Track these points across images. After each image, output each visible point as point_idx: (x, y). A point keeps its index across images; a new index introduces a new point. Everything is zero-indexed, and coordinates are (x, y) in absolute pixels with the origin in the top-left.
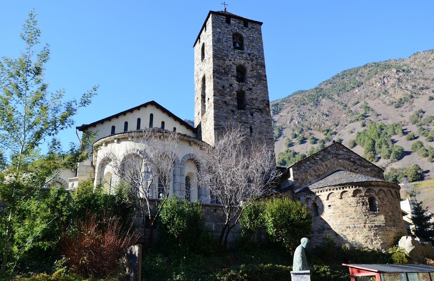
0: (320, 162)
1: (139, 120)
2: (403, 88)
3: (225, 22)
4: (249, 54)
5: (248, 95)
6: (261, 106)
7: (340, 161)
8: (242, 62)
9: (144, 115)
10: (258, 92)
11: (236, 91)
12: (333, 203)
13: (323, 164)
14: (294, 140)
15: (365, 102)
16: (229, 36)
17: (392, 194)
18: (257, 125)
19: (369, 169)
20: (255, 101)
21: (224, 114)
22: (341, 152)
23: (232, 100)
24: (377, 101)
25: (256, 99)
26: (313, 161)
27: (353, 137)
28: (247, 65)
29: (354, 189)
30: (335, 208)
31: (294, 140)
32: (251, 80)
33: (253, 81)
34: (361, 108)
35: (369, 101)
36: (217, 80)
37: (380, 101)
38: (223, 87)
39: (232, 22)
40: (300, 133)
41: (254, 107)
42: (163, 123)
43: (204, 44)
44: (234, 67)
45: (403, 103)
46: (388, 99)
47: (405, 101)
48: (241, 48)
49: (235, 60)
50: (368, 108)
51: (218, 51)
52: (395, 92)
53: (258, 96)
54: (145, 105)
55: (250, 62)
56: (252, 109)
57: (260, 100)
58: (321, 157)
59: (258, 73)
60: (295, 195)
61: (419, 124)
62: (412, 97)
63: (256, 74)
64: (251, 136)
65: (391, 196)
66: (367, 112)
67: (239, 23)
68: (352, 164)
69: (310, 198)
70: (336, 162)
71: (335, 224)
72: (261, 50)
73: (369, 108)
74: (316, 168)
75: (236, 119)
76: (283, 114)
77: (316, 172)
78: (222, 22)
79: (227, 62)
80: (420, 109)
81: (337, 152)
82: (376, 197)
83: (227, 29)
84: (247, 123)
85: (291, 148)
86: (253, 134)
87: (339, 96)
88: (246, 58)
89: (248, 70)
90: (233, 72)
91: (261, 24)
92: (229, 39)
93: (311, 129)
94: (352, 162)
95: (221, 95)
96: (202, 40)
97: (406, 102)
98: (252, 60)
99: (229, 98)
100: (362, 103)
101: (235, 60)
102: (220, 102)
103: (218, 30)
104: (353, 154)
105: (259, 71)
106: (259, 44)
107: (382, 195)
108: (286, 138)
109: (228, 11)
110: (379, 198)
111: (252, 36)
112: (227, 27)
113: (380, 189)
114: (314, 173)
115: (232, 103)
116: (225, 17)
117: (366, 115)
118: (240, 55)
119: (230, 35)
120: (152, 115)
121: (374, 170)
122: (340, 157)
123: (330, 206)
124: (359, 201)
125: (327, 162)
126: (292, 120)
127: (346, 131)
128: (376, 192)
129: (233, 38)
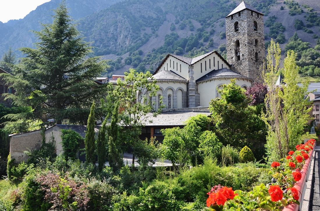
3: (251, 14)
4: (259, 33)
5: (259, 55)
8: (257, 38)
16: (252, 23)
31: (177, 26)
32: (259, 47)
36: (249, 47)
39: (253, 14)
40: (182, 20)
41: (261, 61)
42: (218, 61)
45: (262, 8)
47: (264, 6)
56: (260, 62)
59: (262, 43)
61: (272, 27)
62: (269, 4)
67: (256, 15)
76: (168, 2)
79: (252, 38)
80: (273, 15)
83: (252, 19)
88: (258, 35)
90: (254, 43)
95: (251, 55)
96: (235, 20)
97: (264, 7)
98: (260, 36)
99: (253, 56)
103: (249, 19)
108: (170, 23)
112: (252, 18)
116: (251, 12)
118: (256, 34)
120: (214, 57)
126: (176, 7)
127: (219, 24)
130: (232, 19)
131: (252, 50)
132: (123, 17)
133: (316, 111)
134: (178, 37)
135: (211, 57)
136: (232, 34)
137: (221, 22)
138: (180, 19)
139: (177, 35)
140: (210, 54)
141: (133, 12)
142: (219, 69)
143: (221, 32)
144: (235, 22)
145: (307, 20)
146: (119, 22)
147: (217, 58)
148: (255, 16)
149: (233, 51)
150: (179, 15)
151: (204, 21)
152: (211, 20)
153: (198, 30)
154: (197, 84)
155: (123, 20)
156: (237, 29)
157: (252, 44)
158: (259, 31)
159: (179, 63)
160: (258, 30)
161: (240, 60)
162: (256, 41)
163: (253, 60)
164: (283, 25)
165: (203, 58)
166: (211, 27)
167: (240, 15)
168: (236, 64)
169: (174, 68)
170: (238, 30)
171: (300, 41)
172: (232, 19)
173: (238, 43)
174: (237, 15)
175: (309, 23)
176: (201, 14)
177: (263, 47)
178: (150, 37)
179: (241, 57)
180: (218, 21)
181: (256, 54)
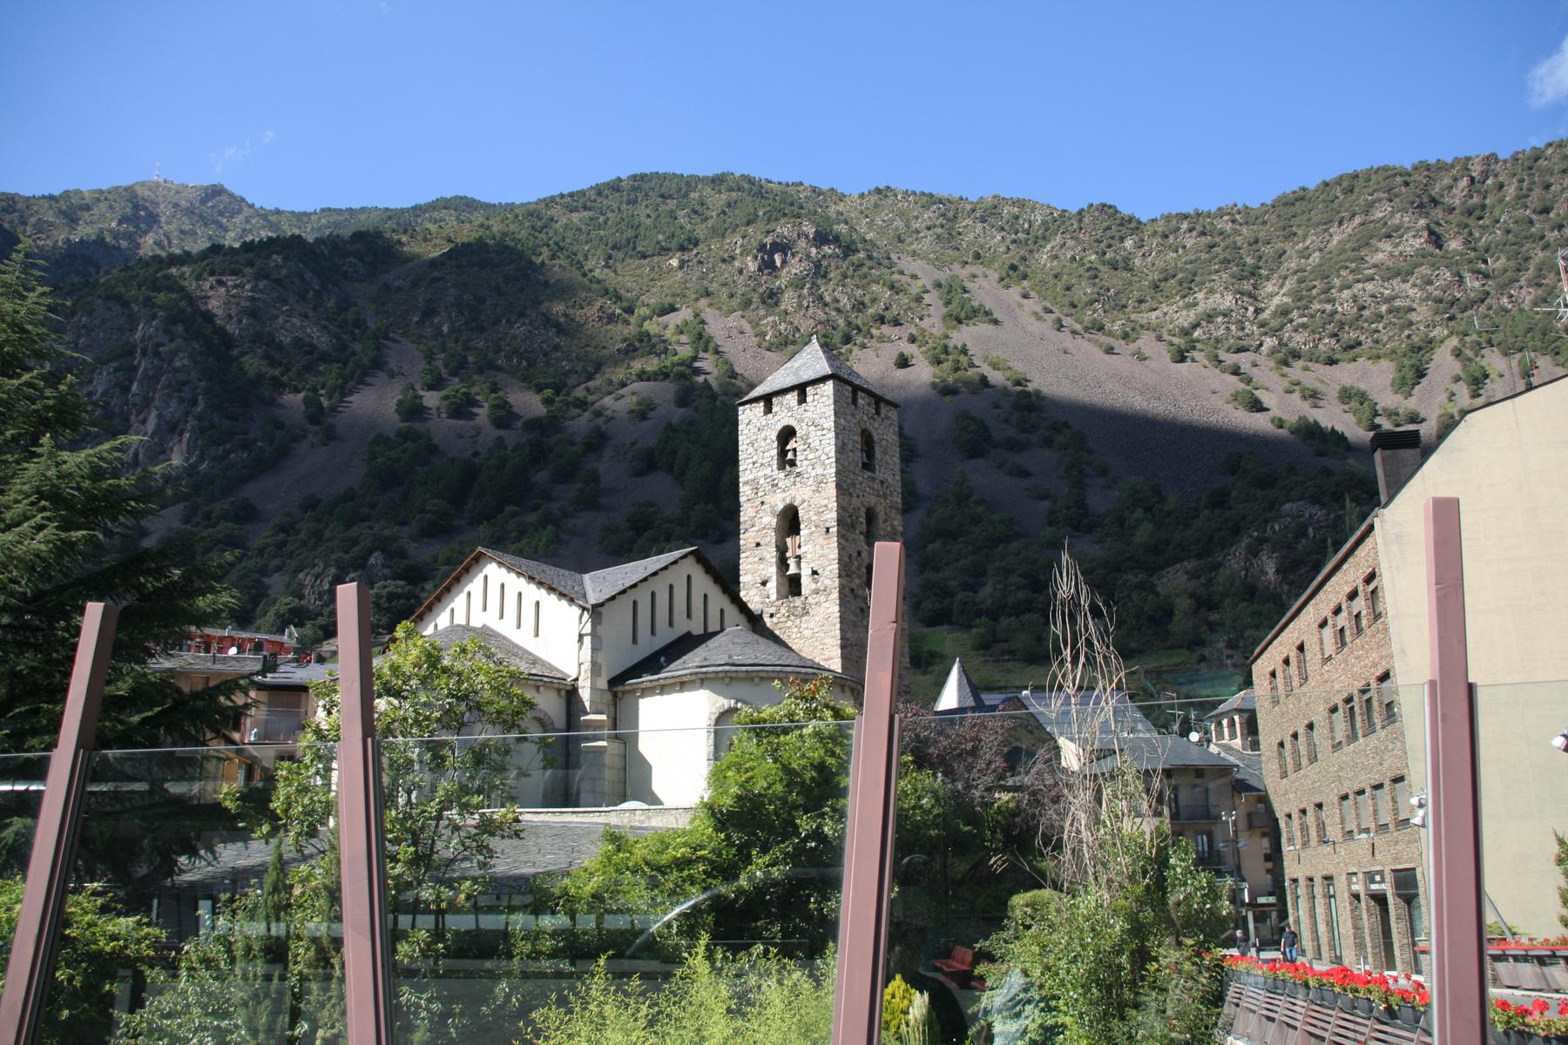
1: (671, 587)
2: (828, 299)
4: (882, 482)
8: (873, 500)
15: (697, 315)
21: (852, 617)
24: (734, 320)
28: (880, 510)
34: (682, 332)
35: (709, 314)
37: (747, 327)
39: (860, 401)
40: (454, 374)
46: (774, 325)
52: (800, 306)
62: (847, 339)
66: (701, 355)
73: (709, 340)
76: (397, 283)
79: (854, 500)
85: (417, 426)
87: (607, 266)
93: (499, 369)
100: (684, 314)
117: (697, 364)
130: (768, 410)
132: (167, 332)
134: (433, 449)
135: (677, 578)
136: (766, 477)
137: (635, 399)
138: (446, 366)
139: (430, 439)
140: (671, 559)
141: (219, 312)
142: (710, 630)
143: (633, 444)
144: (779, 427)
145: (1006, 421)
146: (144, 353)
147: (703, 583)
149: (771, 554)
152: (591, 384)
154: (615, 695)
155: (163, 345)
156: (790, 456)
157: (853, 526)
158: (879, 475)
159: (532, 592)
161: (799, 594)
162: (871, 516)
163: (856, 596)
165: (645, 579)
166: (587, 415)
167: (802, 400)
168: (783, 611)
169: (502, 617)
170: (793, 463)
171: (980, 509)
172: (768, 410)
173: (790, 521)
174: (792, 398)
175: (1012, 432)
176: (545, 355)
178: (295, 439)
179: (804, 580)
180: (622, 391)
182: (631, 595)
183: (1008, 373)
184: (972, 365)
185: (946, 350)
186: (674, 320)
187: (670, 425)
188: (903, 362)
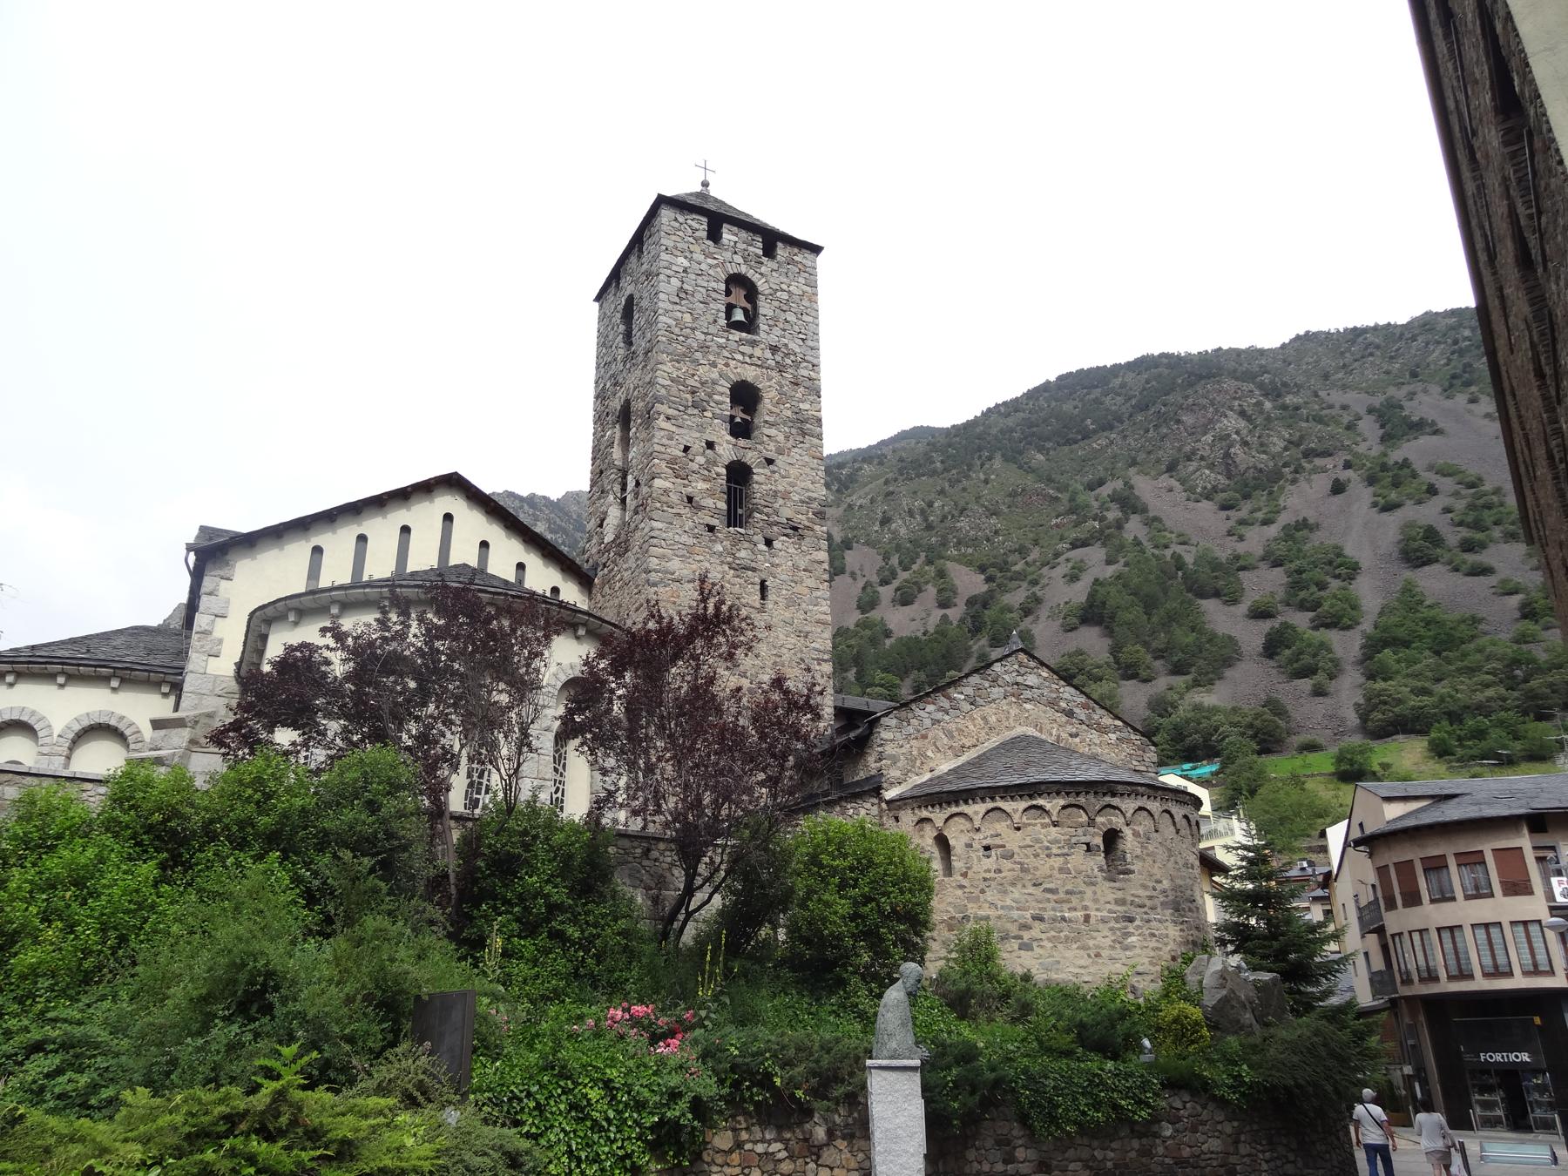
0: (966, 707)
4: (774, 349)
6: (802, 519)
7: (1028, 706)
8: (750, 374)
9: (425, 517)
10: (793, 471)
11: (727, 467)
12: (998, 841)
13: (977, 714)
14: (886, 592)
17: (1174, 824)
18: (783, 577)
19: (1113, 736)
20: (781, 501)
22: (1031, 680)
23: (711, 493)
24: (1166, 481)
25: (786, 496)
26: (946, 704)
27: (1078, 593)
29: (1062, 802)
30: (1003, 857)
32: (772, 432)
33: (781, 438)
38: (686, 449)
40: (905, 569)
43: (630, 299)
44: (724, 388)
47: (1256, 488)
48: (749, 325)
49: (727, 365)
50: (1128, 503)
51: (677, 331)
53: (790, 484)
54: (426, 489)
55: (774, 374)
57: (796, 498)
58: (969, 691)
60: (884, 805)
61: (1293, 566)
63: (789, 413)
64: (762, 610)
65: (1172, 829)
68: (1065, 719)
69: (928, 820)
70: (1014, 711)
71: (1000, 904)
72: (809, 337)
74: (952, 726)
75: (721, 554)
77: (950, 735)
78: (697, 234)
81: (1020, 679)
82: (1127, 832)
83: (710, 261)
84: (754, 570)
86: (770, 605)
89: (766, 401)
91: (816, 249)
92: (714, 295)
94: (1063, 711)
96: (628, 287)
98: (781, 369)
99: (701, 485)
101: (727, 365)
102: (674, 498)
103: (681, 260)
104: (1068, 689)
105: (802, 406)
106: (805, 318)
107: (1144, 824)
108: (861, 584)
109: (714, 192)
110: (1136, 834)
111: (784, 287)
113: (1141, 809)
114: (946, 740)
115: (709, 502)
116: (705, 219)
118: (747, 349)
119: (717, 281)
120: (448, 518)
121: (1129, 741)
122: (1028, 694)
123: (987, 848)
124: (1074, 840)
125: (989, 710)
128: (1129, 815)
129: (728, 293)
131: (698, 446)
133: (1405, 906)
137: (1070, 565)
138: (900, 563)
148: (741, 246)
150: (898, 548)
151: (1004, 567)
153: (971, 602)
158: (767, 334)
160: (763, 327)
164: (1349, 551)
166: (1025, 585)
176: (988, 540)
177: (804, 434)
181: (739, 474)
182: (323, 539)
183: (1458, 478)
184: (1414, 475)
185: (1384, 467)
186: (1105, 491)
187: (1097, 580)
188: (1338, 488)
